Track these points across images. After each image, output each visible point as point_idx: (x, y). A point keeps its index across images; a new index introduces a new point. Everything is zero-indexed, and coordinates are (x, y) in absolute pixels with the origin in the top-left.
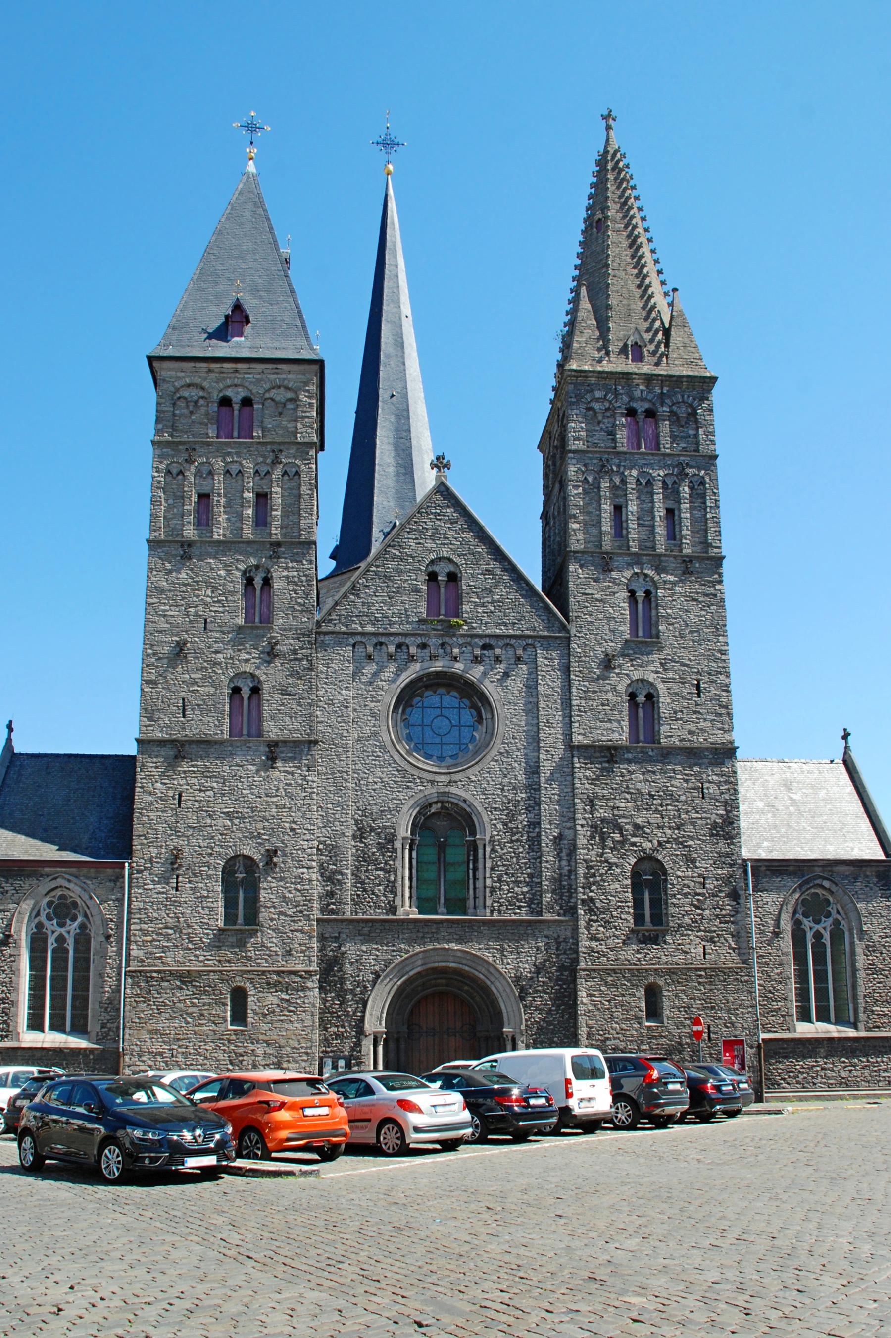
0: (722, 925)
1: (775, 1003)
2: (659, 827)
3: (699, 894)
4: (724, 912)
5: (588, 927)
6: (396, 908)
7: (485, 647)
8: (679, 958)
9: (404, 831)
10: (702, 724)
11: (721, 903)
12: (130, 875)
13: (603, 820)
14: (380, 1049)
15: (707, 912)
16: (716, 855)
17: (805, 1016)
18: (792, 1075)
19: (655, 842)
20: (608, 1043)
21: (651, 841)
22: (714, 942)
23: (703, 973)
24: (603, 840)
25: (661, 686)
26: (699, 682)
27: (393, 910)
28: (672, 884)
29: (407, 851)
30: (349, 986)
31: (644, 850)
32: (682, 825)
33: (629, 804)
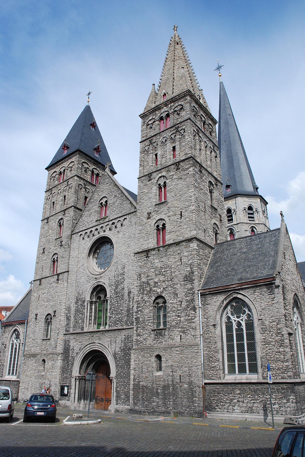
0: (189, 324)
1: (213, 363)
2: (164, 281)
3: (179, 310)
4: (189, 318)
5: (136, 331)
6: (83, 327)
7: (113, 223)
8: (171, 342)
9: (88, 298)
10: (182, 231)
11: (188, 313)
12: (27, 323)
13: (143, 282)
14: (77, 383)
15: (182, 319)
16: (186, 290)
17: (232, 370)
18: (222, 404)
19: (162, 289)
20: (141, 383)
21: (160, 288)
22: (185, 333)
23: (178, 349)
24: (144, 291)
25: (167, 219)
26: (181, 212)
27: (82, 329)
28: (168, 307)
29: (89, 306)
30: (70, 359)
31: (158, 293)
32: (173, 278)
33: (153, 274)
